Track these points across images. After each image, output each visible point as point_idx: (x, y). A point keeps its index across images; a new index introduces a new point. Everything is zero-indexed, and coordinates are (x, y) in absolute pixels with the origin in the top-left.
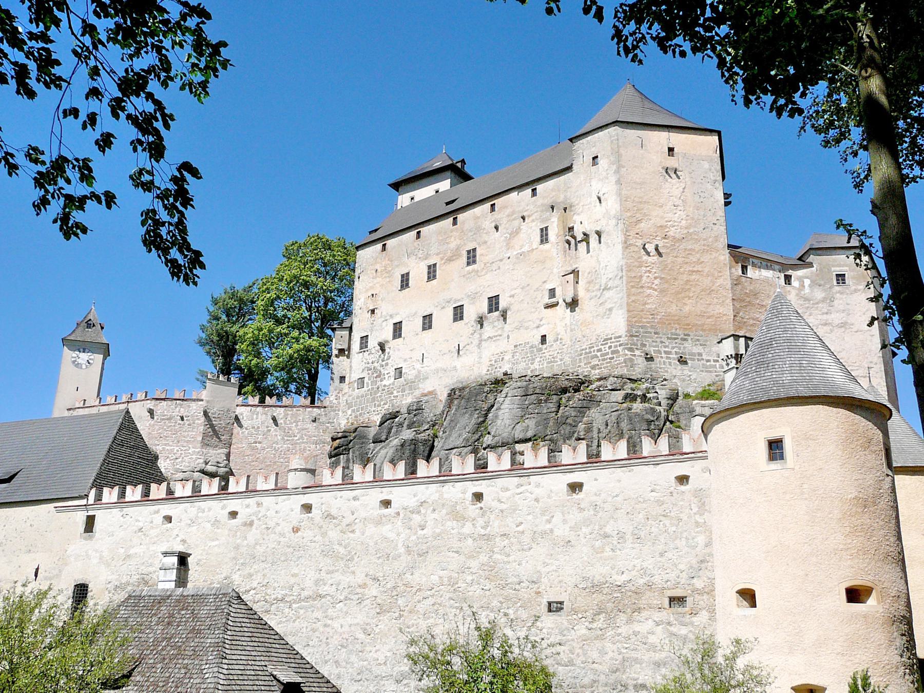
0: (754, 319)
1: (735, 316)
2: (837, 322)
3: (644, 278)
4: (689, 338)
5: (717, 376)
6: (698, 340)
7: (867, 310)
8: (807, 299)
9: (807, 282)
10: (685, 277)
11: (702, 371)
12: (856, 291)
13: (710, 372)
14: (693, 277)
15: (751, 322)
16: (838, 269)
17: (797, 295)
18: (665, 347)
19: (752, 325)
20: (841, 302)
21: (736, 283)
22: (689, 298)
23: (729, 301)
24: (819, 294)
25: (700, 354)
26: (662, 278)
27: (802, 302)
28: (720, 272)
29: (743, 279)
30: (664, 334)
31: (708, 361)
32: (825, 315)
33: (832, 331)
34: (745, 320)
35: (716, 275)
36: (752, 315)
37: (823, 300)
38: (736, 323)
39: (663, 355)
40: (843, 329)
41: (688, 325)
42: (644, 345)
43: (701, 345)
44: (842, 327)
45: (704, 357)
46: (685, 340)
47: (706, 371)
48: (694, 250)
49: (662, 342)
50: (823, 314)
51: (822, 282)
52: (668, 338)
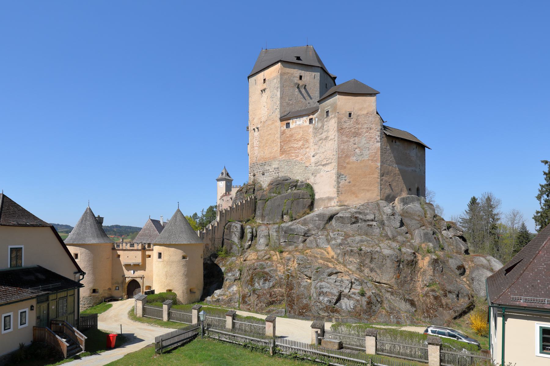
0: (290, 148)
1: (281, 149)
2: (324, 137)
3: (255, 143)
4: (266, 164)
5: (273, 177)
6: (269, 164)
7: (334, 128)
8: (316, 129)
9: (317, 119)
10: (266, 138)
11: (269, 177)
12: (332, 118)
13: (271, 176)
14: (268, 137)
15: (289, 149)
16: (326, 109)
17: (313, 128)
18: (259, 170)
19: (289, 151)
20: (326, 126)
21: (283, 133)
22: (267, 146)
23: (279, 144)
24: (320, 125)
25: (269, 170)
26: (259, 141)
27: (314, 131)
28: (277, 131)
29: (286, 130)
30: (259, 165)
31: (271, 172)
32: (321, 135)
33: (322, 142)
34: (286, 149)
35: (275, 133)
36: (289, 146)
37: (321, 128)
38: (281, 152)
39: (259, 173)
40: (326, 140)
41: (266, 158)
42: (254, 171)
43: (269, 166)
44: (325, 139)
45: (270, 171)
46: (265, 165)
47: (270, 177)
48: (269, 125)
49: (258, 168)
50: (320, 134)
51: (321, 118)
52: (260, 166)
